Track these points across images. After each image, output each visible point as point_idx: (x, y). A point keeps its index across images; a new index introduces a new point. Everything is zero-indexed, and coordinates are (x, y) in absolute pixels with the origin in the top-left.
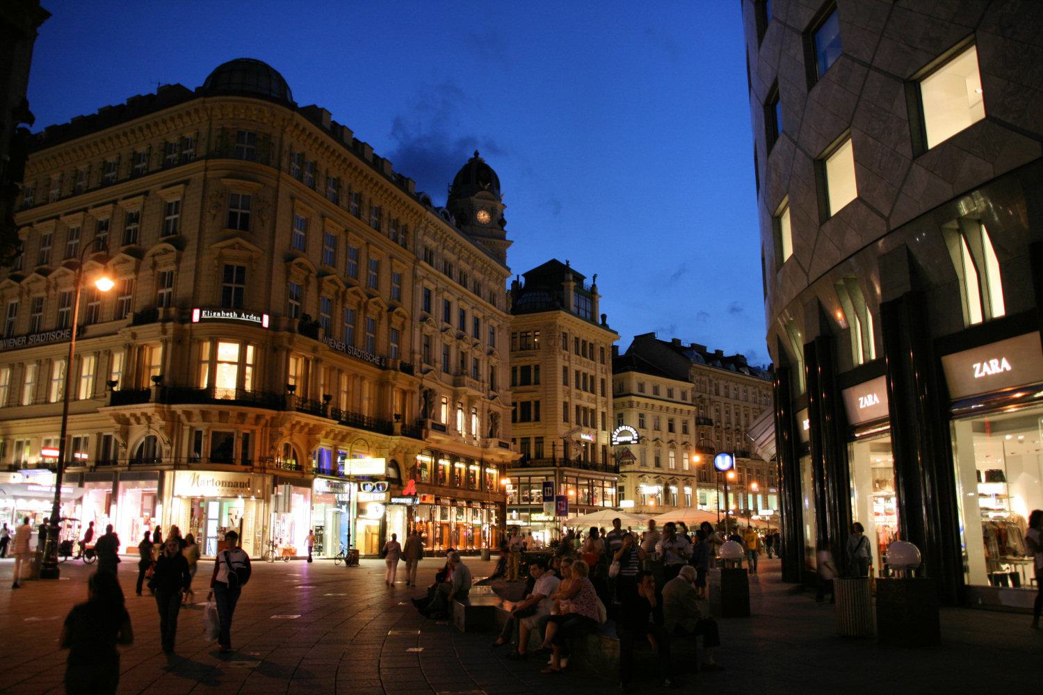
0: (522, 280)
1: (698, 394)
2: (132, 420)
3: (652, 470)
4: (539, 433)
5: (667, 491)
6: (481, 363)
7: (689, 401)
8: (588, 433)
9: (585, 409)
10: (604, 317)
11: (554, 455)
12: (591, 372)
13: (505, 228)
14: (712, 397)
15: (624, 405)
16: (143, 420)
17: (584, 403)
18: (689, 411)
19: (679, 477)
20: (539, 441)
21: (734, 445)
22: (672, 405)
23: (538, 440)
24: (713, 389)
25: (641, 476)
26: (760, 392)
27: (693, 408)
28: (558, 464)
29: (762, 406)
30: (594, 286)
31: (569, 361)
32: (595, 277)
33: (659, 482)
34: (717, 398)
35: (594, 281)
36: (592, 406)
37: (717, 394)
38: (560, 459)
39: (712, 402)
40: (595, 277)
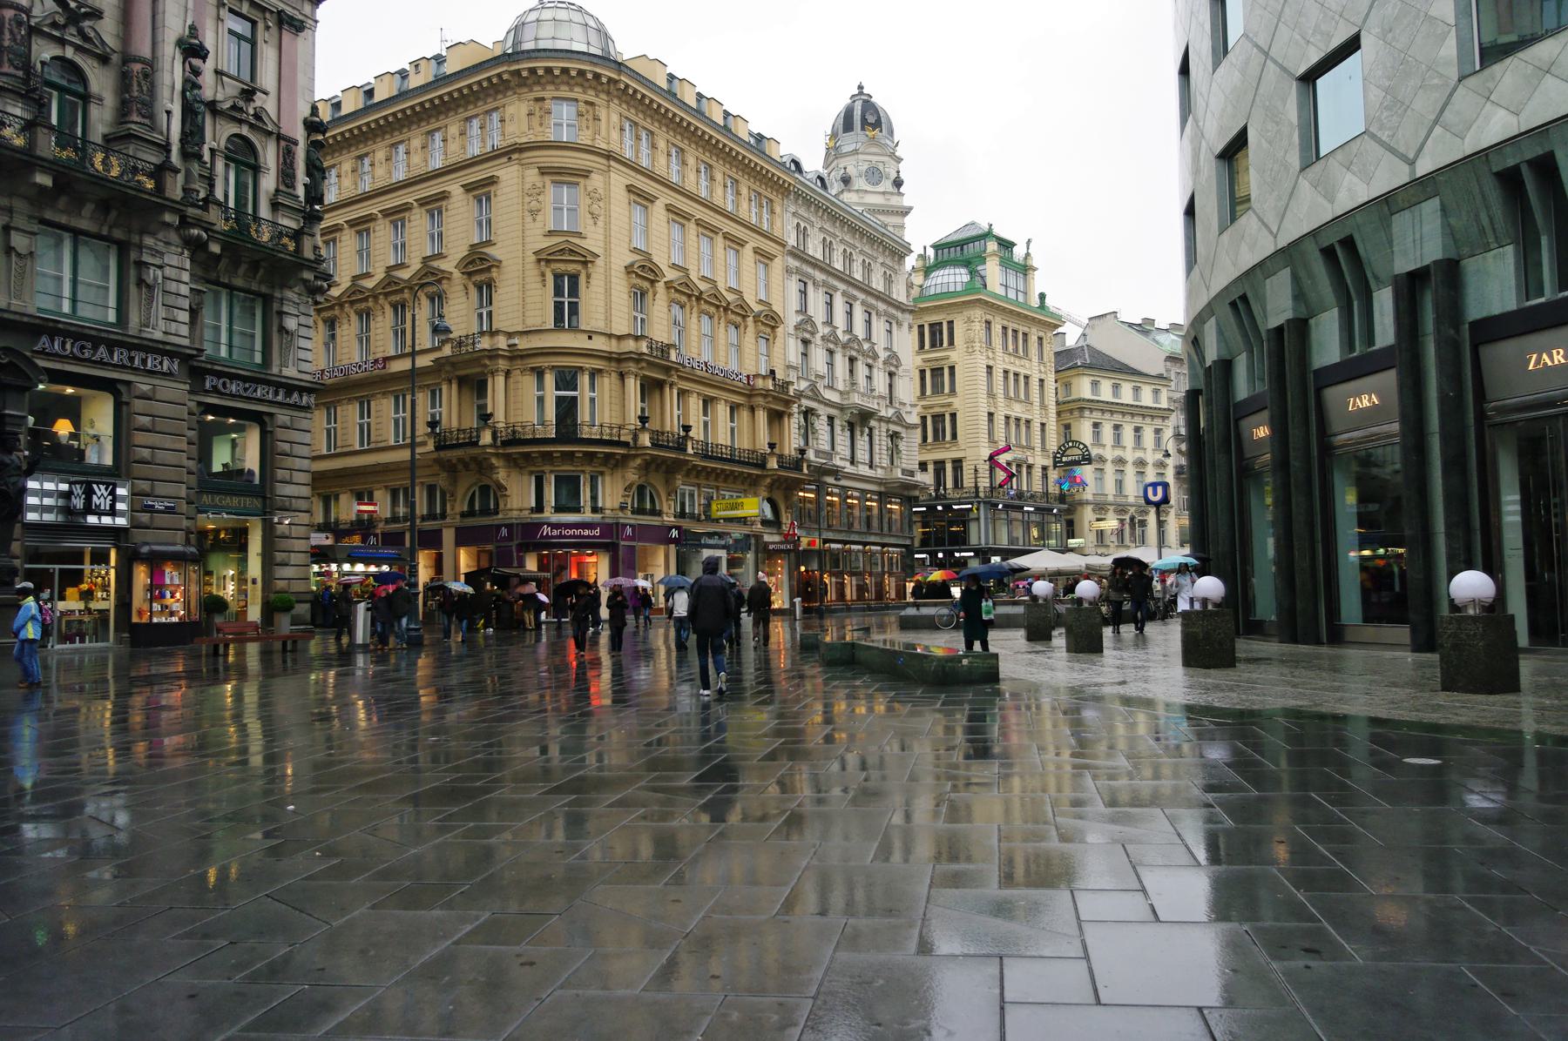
0: (931, 253)
2: (460, 467)
9: (1018, 420)
10: (1042, 296)
12: (1023, 371)
13: (902, 190)
16: (473, 466)
20: (958, 464)
30: (1028, 254)
36: (1024, 416)
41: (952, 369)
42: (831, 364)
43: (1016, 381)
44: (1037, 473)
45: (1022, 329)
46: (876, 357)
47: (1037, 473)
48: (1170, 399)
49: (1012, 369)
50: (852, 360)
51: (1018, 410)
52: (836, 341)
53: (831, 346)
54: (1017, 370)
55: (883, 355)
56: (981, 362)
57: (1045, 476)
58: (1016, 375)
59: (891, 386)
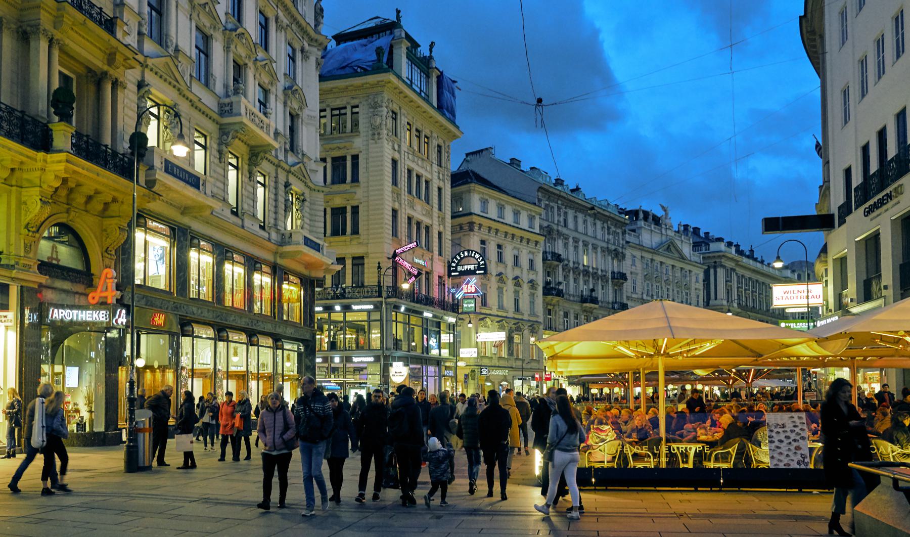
1: (545, 224)
3: (494, 312)
4: (358, 251)
5: (510, 339)
6: (272, 98)
7: (537, 230)
8: (422, 257)
11: (379, 282)
14: (560, 228)
15: (461, 228)
17: (418, 215)
18: (537, 243)
19: (524, 323)
20: (359, 261)
21: (581, 289)
22: (518, 233)
23: (357, 262)
24: (562, 219)
25: (482, 319)
26: (609, 228)
27: (541, 239)
28: (384, 294)
29: (610, 246)
31: (399, 152)
32: (432, 45)
33: (502, 328)
34: (565, 231)
35: (431, 51)
36: (426, 221)
37: (565, 225)
38: (388, 287)
39: (559, 234)
40: (432, 45)
41: (355, 158)
42: (204, 50)
43: (418, 183)
44: (435, 280)
45: (426, 131)
46: (273, 76)
47: (435, 280)
48: (541, 227)
49: (417, 169)
50: (239, 69)
51: (418, 214)
52: (213, 16)
53: (206, 22)
54: (422, 171)
55: (282, 83)
56: (388, 153)
57: (442, 284)
58: (418, 177)
59: (292, 129)
